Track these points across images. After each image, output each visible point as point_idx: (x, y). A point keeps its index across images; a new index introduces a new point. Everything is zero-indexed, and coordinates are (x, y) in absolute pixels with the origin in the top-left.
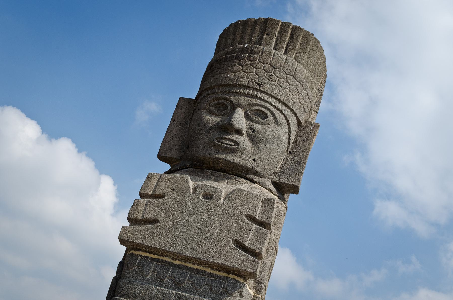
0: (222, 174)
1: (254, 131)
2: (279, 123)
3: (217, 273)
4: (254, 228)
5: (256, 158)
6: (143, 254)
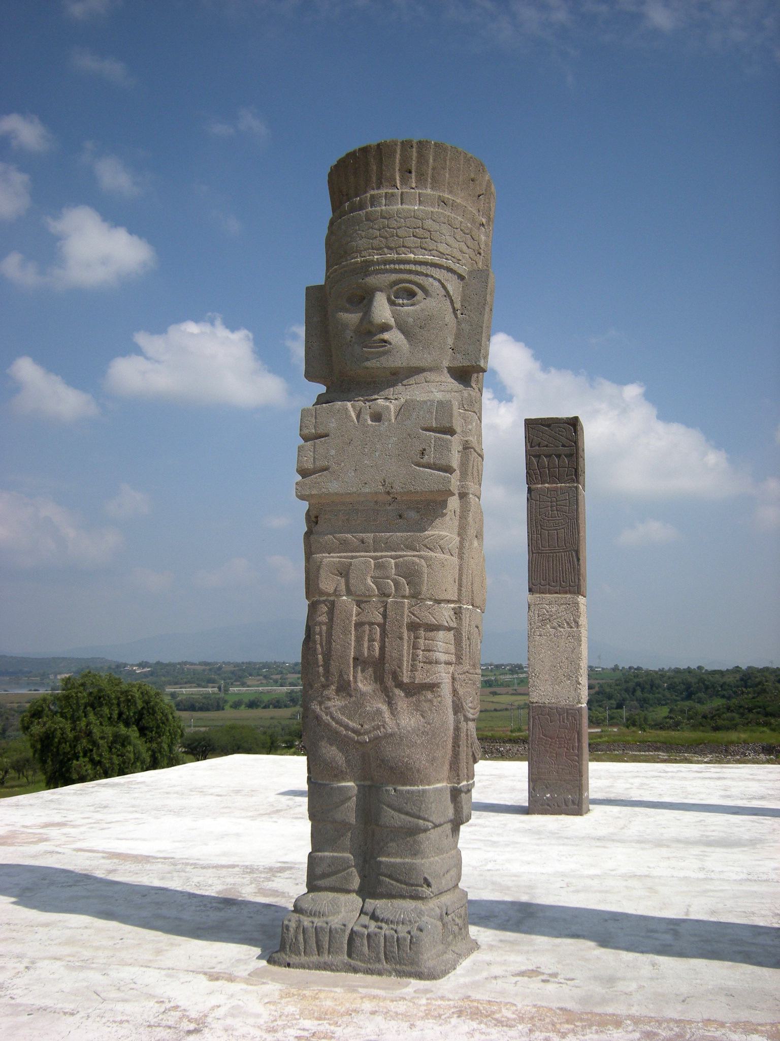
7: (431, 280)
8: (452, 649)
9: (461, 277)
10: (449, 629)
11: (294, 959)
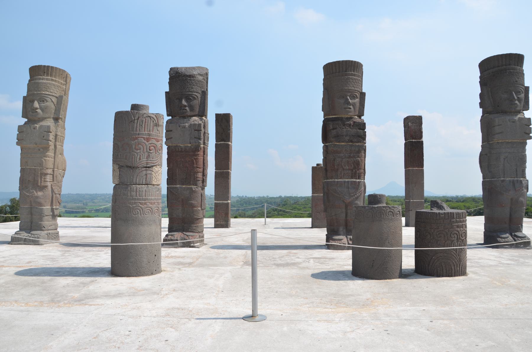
0: (512, 113)
6: (500, 141)
7: (48, 98)
8: (52, 178)
9: (56, 97)
10: (51, 174)
11: (13, 243)
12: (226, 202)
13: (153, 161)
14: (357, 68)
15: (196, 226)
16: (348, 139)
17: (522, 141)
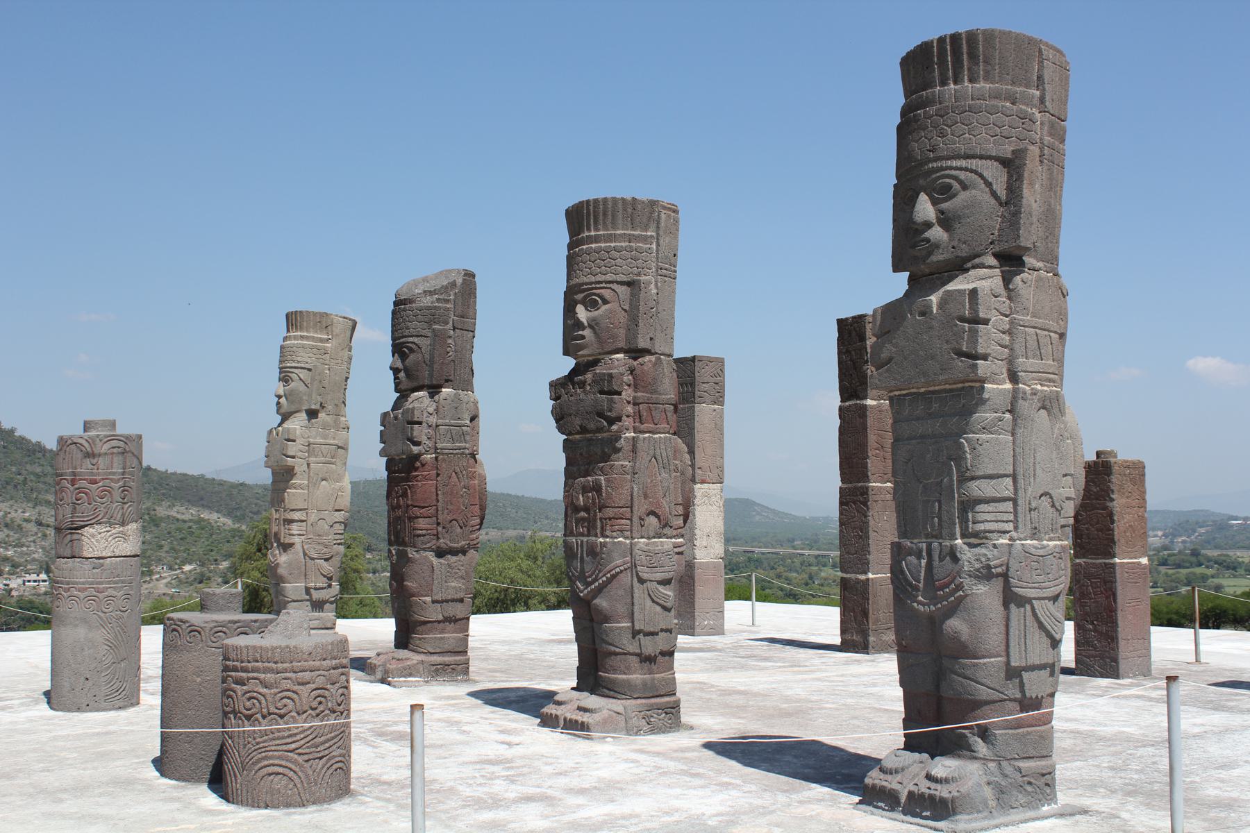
1: (942, 212)
2: (968, 184)
3: (955, 386)
4: (967, 329)
5: (955, 243)
6: (897, 393)
12: (862, 577)
13: (83, 517)
14: (605, 214)
15: (420, 639)
16: (579, 423)
17: (960, 385)
